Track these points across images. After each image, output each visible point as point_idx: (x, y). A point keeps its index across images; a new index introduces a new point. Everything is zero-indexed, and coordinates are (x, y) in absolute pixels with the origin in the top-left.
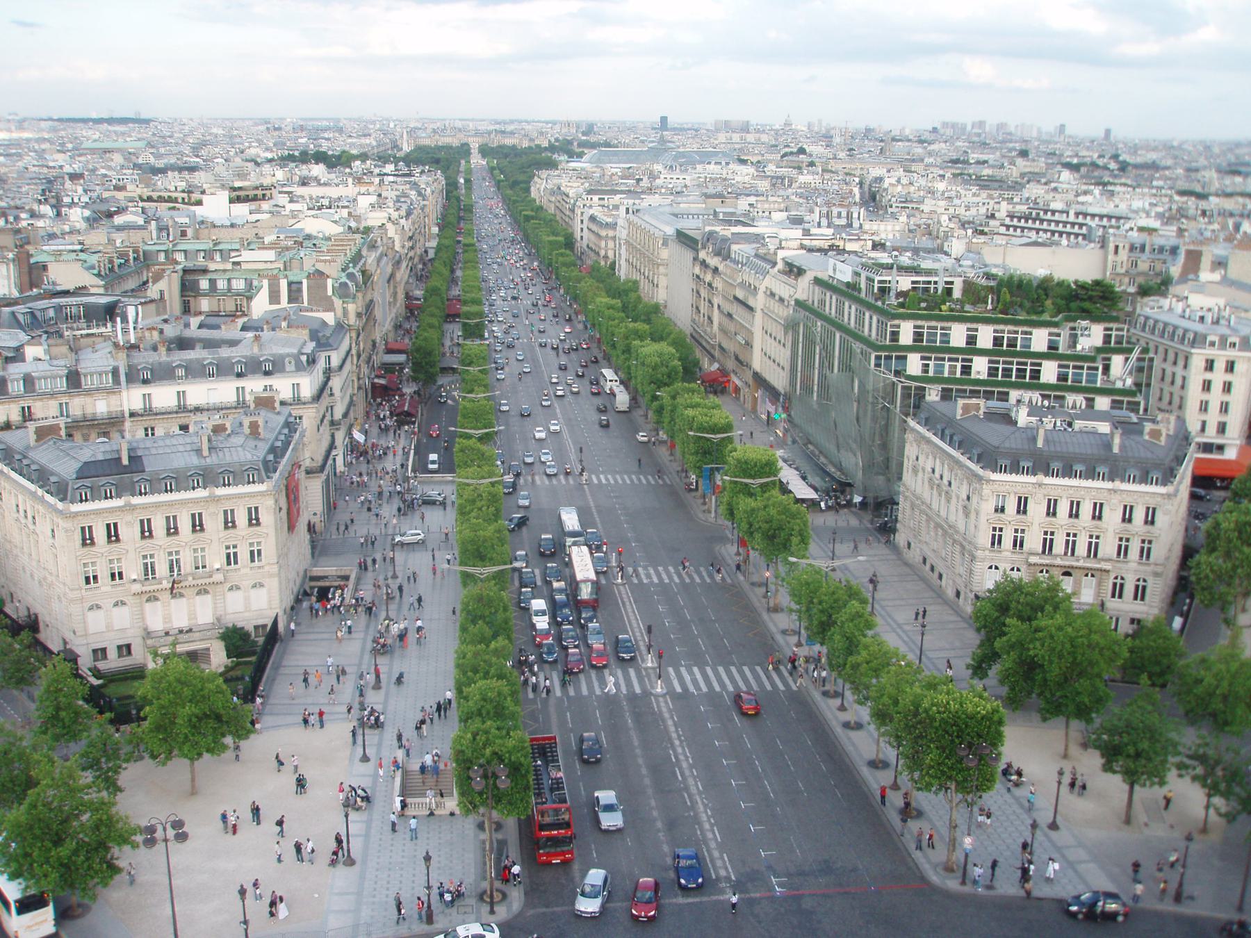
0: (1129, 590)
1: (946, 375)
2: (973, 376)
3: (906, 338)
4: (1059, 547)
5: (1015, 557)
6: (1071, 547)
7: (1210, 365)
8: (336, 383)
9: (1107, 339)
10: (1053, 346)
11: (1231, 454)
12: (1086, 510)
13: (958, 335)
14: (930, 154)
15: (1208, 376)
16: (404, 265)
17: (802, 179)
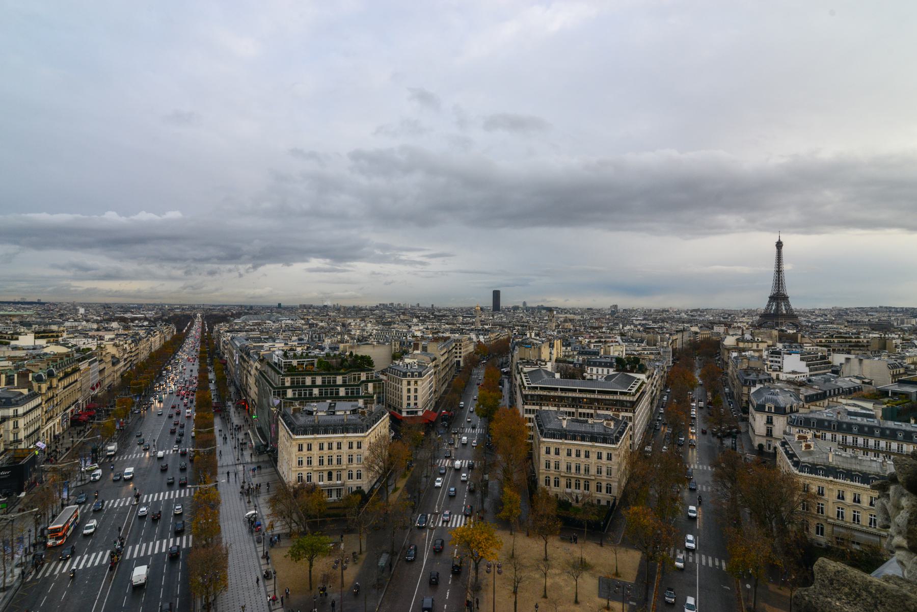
0: (355, 476)
1: (303, 396)
2: (314, 396)
3: (288, 384)
4: (326, 462)
5: (308, 468)
6: (330, 461)
7: (409, 384)
8: (22, 422)
9: (367, 378)
10: (344, 381)
11: (420, 414)
12: (335, 446)
13: (308, 381)
14: (372, 315)
15: (409, 387)
16: (122, 363)
17: (321, 324)
